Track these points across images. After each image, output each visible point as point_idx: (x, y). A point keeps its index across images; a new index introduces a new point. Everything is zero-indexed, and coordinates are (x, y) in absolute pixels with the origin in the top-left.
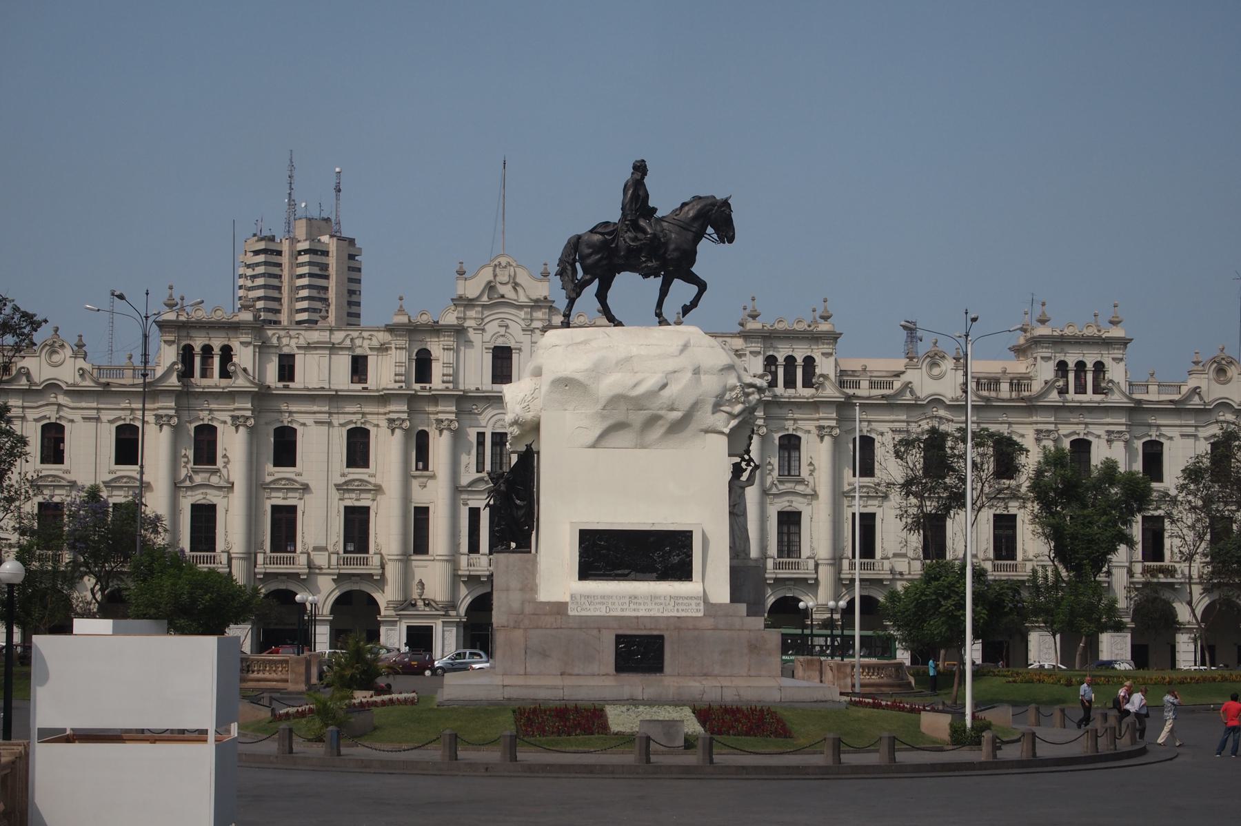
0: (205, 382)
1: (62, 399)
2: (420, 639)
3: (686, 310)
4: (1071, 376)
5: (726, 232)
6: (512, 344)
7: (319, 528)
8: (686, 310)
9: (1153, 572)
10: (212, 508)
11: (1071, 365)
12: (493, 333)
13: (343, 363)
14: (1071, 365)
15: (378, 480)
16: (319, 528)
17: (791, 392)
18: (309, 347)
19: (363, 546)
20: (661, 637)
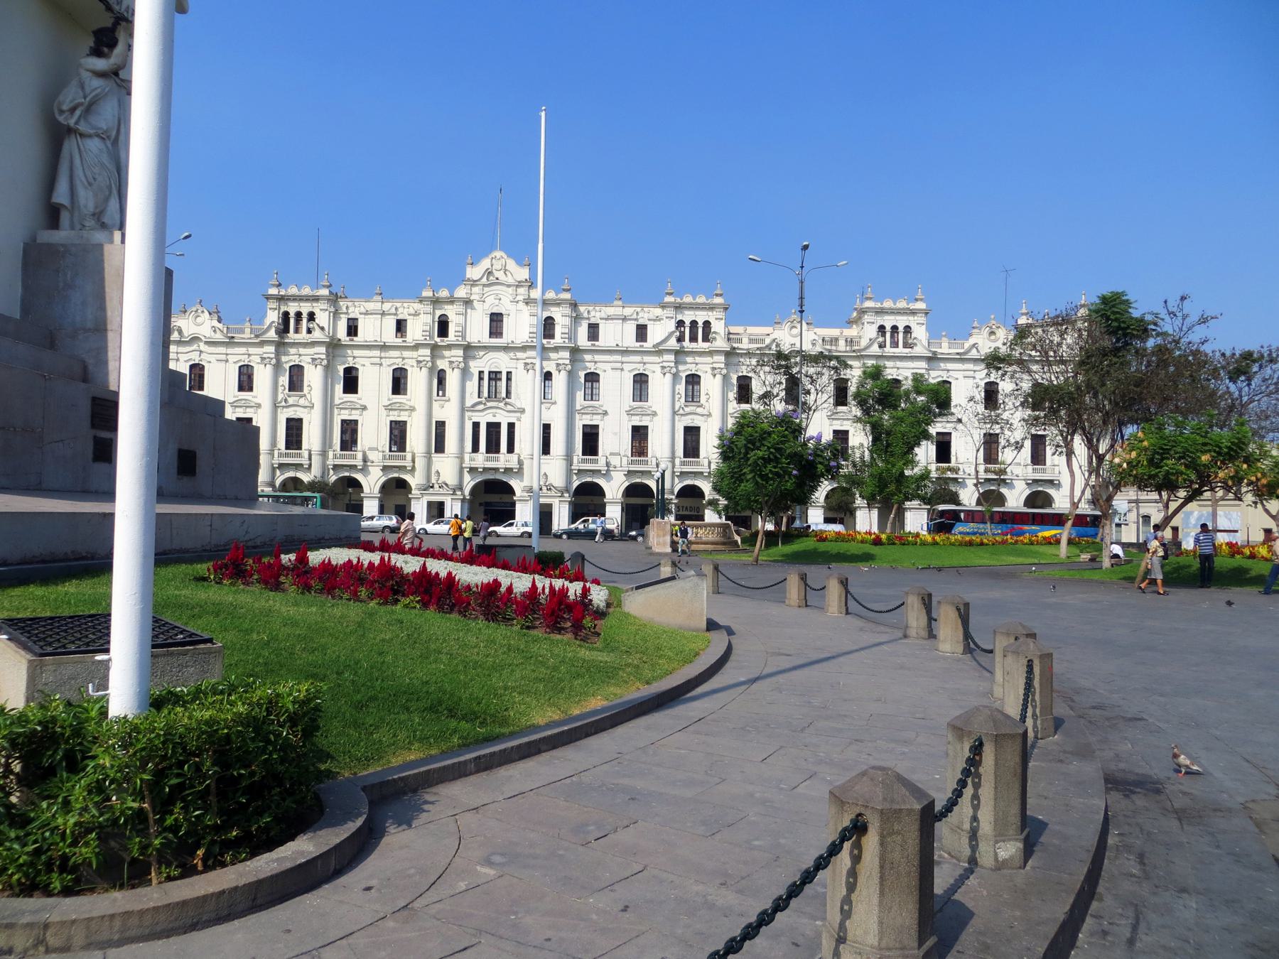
0: (297, 336)
1: (203, 347)
4: (888, 335)
7: (373, 436)
9: (944, 470)
10: (300, 420)
11: (888, 328)
12: (491, 305)
14: (888, 328)
15: (411, 403)
16: (373, 436)
17: (694, 345)
18: (366, 313)
19: (402, 448)
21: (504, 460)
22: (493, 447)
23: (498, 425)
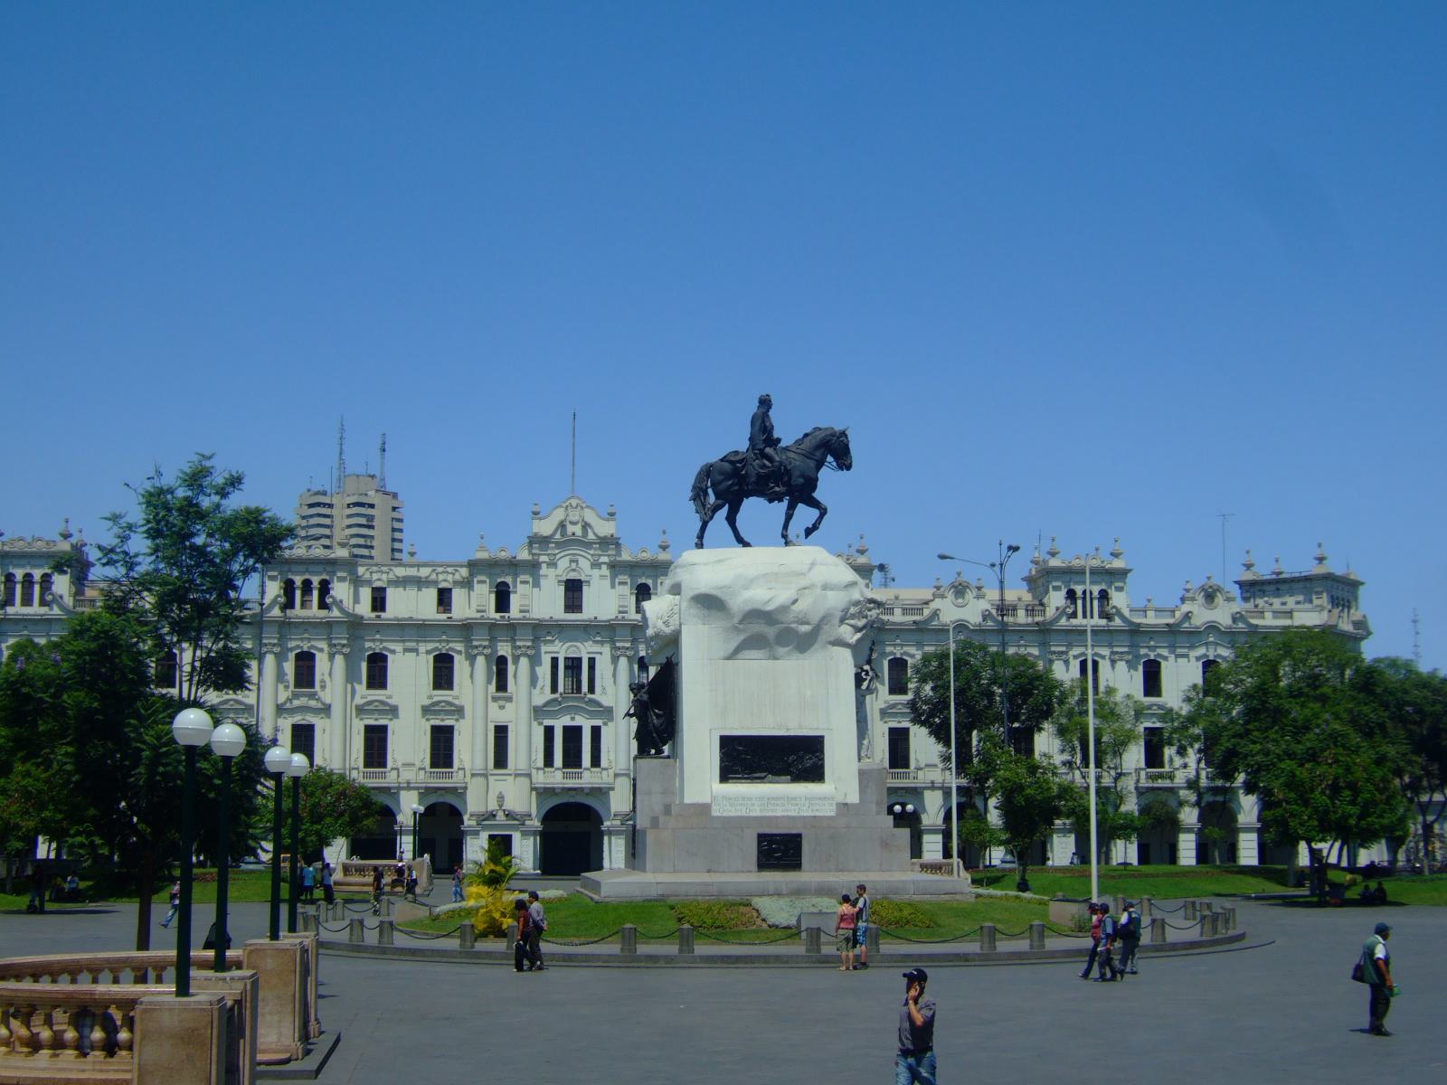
0: (305, 613)
2: (501, 846)
3: (808, 532)
4: (1079, 603)
5: (843, 457)
6: (583, 578)
7: (409, 746)
8: (808, 532)
12: (563, 569)
13: (431, 595)
16: (409, 746)
20: (799, 836)
21: (588, 777)
22: (572, 759)
23: (578, 729)
